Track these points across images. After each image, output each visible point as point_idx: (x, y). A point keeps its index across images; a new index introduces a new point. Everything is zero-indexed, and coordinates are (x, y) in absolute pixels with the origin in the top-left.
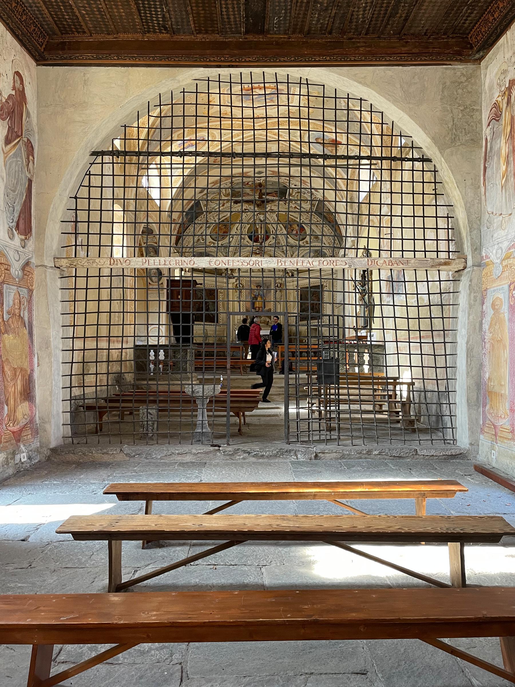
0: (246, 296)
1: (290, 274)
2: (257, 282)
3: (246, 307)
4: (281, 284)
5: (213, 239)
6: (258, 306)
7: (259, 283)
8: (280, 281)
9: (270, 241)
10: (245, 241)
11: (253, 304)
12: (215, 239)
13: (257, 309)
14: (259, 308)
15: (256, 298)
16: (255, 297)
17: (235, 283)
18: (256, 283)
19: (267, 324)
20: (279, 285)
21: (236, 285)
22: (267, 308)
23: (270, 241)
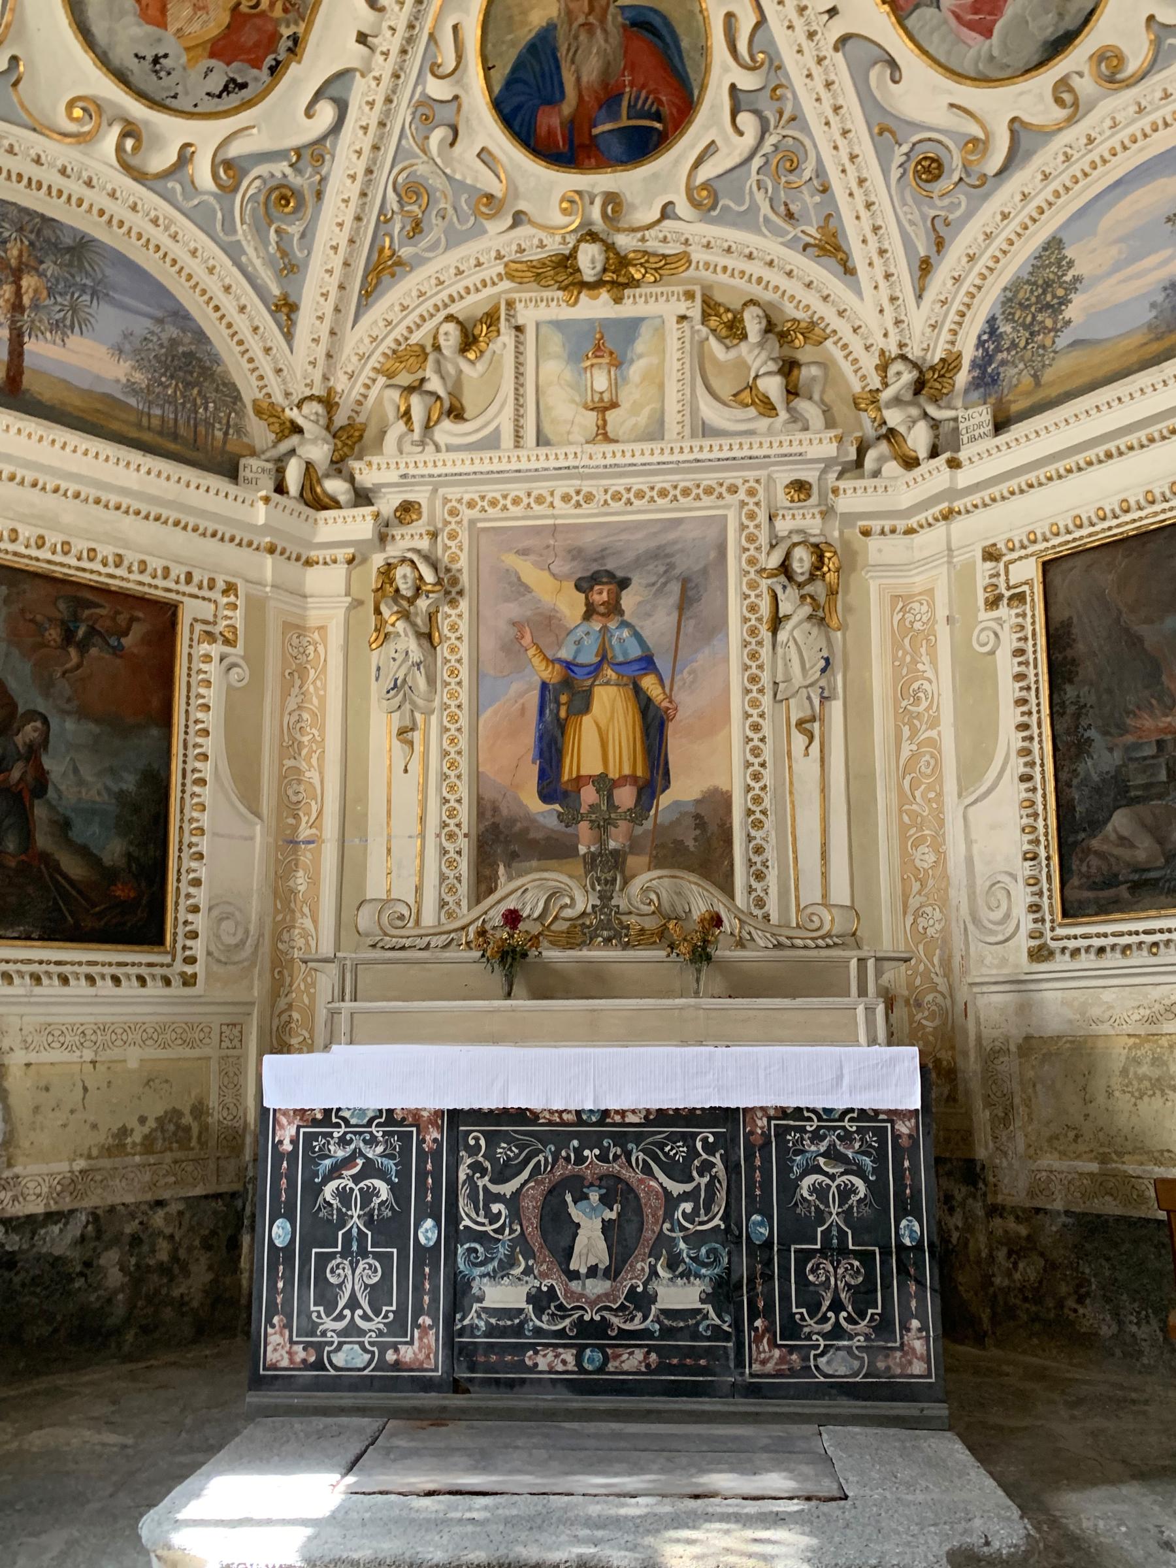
0: (478, 674)
1: (919, 439)
2: (588, 540)
3: (477, 777)
4: (818, 552)
5: (121, 77)
6: (591, 765)
7: (602, 554)
8: (813, 525)
9: (710, 149)
10: (467, 150)
11: (551, 750)
12: (149, 83)
13: (589, 795)
14: (605, 784)
15: (564, 698)
16: (567, 684)
17: (378, 560)
18: (576, 553)
19: (701, 955)
20: (802, 561)
21: (387, 571)
22: (684, 789)
23: (710, 149)
